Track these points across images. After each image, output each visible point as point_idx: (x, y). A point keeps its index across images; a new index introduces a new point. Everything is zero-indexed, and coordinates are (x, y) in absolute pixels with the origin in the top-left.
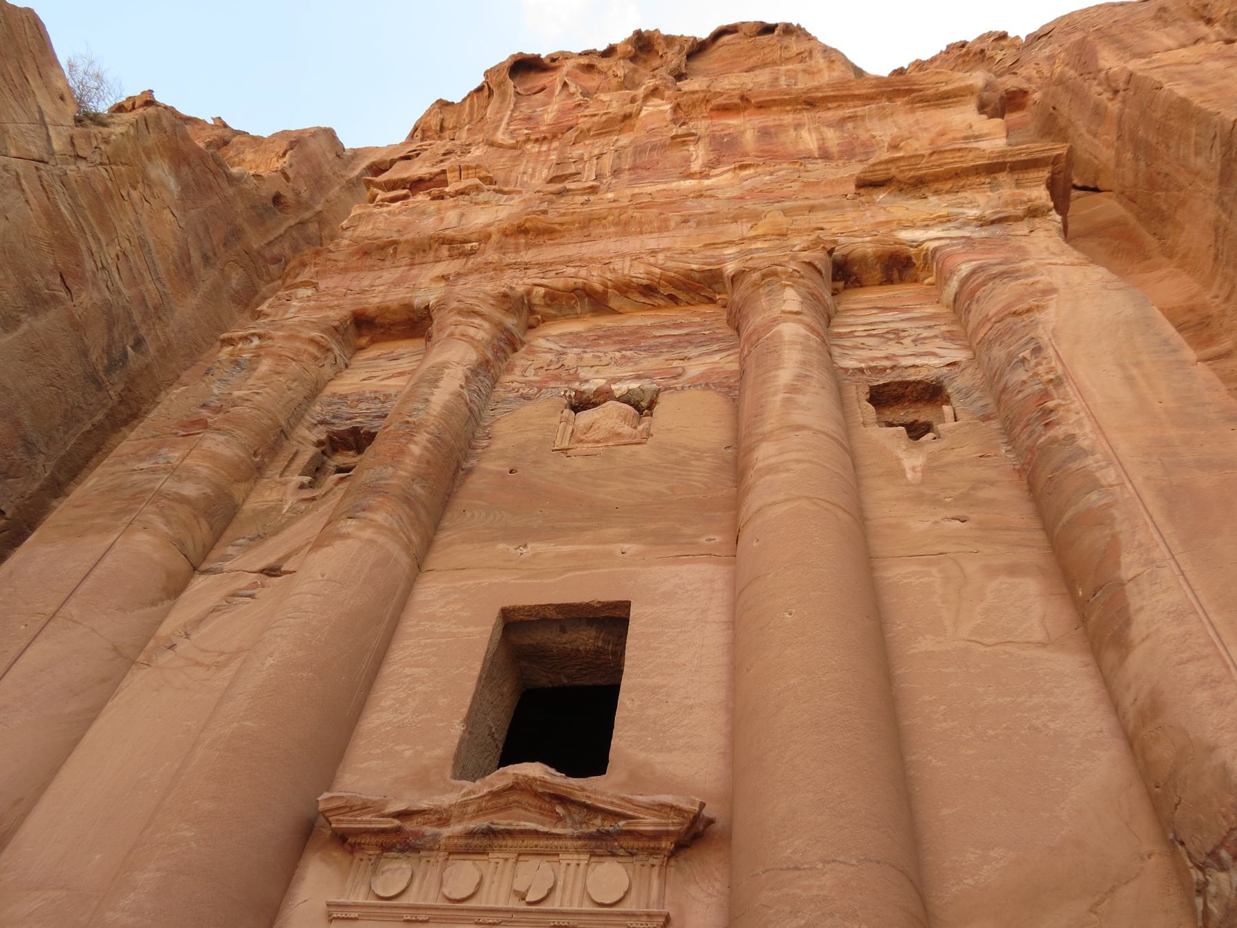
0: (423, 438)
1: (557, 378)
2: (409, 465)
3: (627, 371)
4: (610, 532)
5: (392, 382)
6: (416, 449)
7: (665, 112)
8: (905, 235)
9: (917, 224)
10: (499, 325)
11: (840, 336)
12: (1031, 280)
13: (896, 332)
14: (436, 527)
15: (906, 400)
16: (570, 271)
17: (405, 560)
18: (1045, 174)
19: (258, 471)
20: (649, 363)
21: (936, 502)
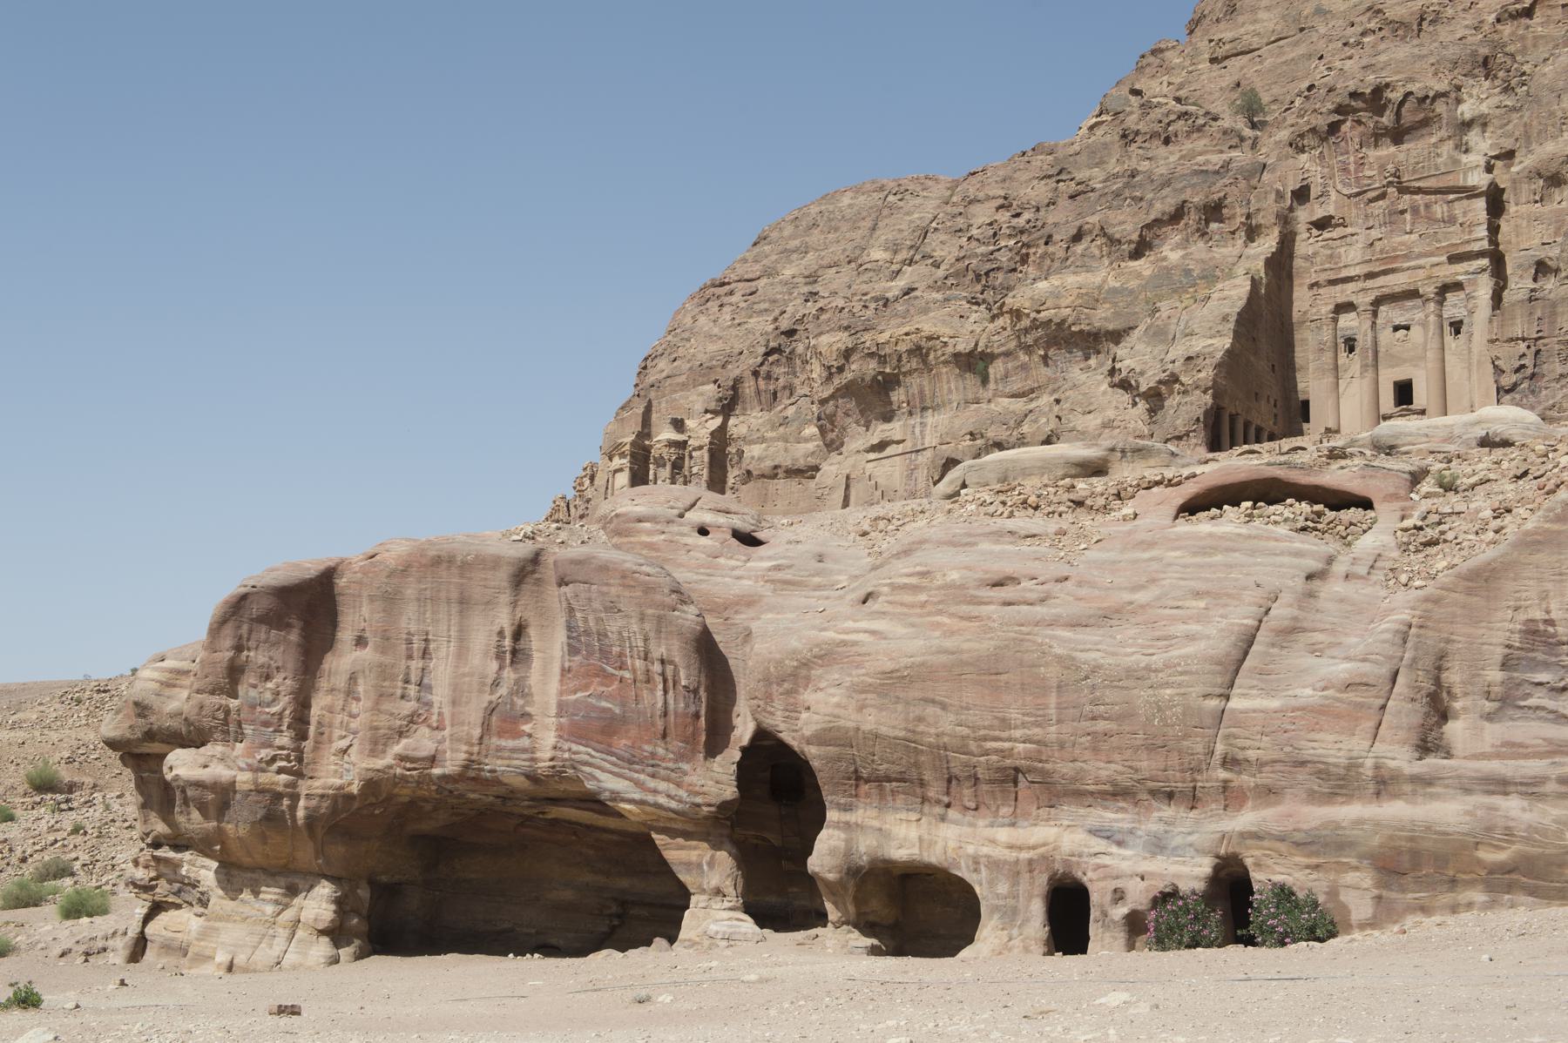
9: (1460, 271)
15: (1457, 327)
20: (1408, 316)
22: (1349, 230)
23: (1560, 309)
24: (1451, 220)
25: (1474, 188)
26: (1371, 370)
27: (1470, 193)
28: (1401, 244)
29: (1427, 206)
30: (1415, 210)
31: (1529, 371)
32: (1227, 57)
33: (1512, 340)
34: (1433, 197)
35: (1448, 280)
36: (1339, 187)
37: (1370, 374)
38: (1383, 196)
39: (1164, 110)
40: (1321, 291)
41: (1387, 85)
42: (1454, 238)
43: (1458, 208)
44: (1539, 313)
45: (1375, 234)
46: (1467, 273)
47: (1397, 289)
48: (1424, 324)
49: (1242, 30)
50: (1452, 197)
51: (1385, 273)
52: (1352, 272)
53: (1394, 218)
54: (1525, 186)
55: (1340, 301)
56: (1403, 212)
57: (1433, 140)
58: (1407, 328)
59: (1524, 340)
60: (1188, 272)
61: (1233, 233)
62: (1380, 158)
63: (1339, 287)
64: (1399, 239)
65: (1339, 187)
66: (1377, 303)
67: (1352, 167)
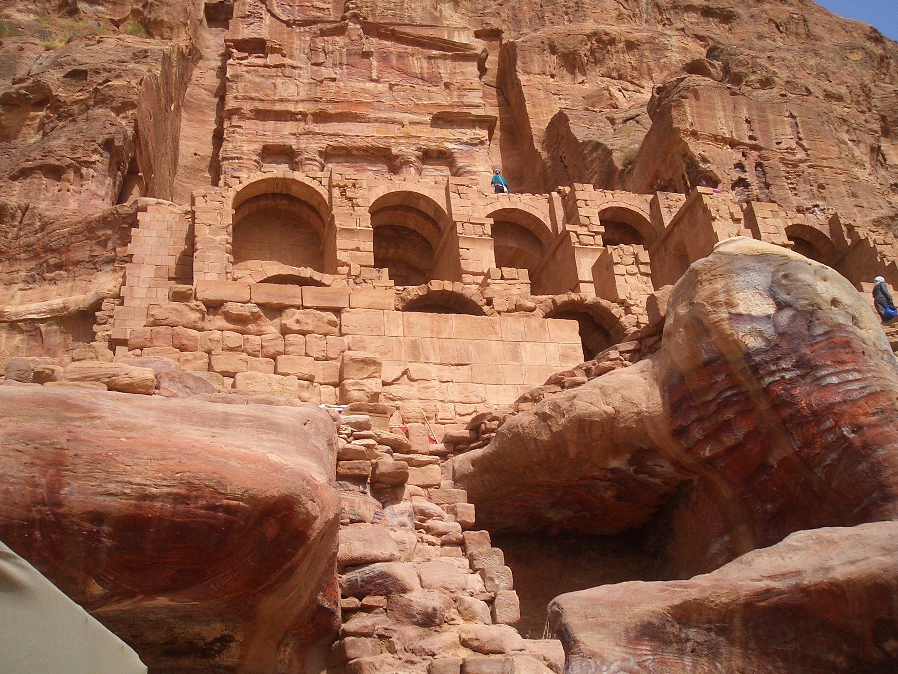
9: (449, 138)
10: (321, 163)
12: (474, 177)
16: (340, 140)
18: (488, 124)
22: (287, 61)
23: (771, 117)
25: (466, 46)
27: (460, 53)
28: (364, 90)
29: (400, 56)
30: (384, 58)
34: (410, 49)
35: (433, 146)
36: (277, 11)
38: (341, 31)
40: (242, 123)
42: (442, 99)
43: (445, 69)
44: (745, 113)
45: (327, 72)
47: (360, 143)
50: (434, 52)
51: (342, 118)
52: (291, 108)
53: (356, 60)
54: (536, 57)
55: (270, 141)
56: (367, 55)
59: (733, 144)
61: (117, 24)
63: (270, 125)
64: (361, 85)
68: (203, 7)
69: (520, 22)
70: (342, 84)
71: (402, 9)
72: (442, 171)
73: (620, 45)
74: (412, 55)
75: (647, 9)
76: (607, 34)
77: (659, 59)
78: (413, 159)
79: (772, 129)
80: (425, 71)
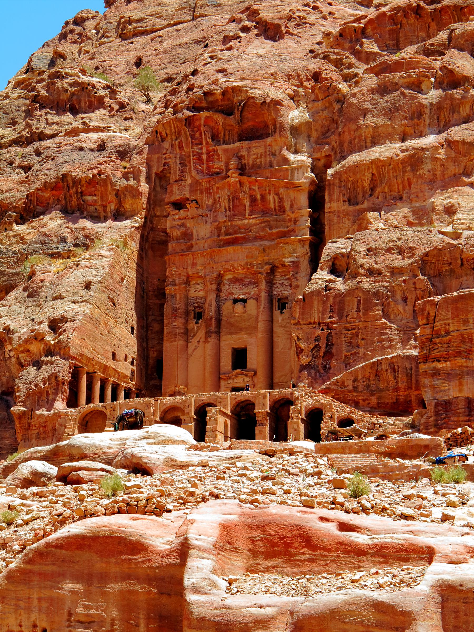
0: (213, 320)
1: (230, 294)
2: (213, 325)
3: (241, 292)
4: (243, 333)
5: (200, 293)
6: (213, 322)
7: (237, 182)
8: (284, 260)
11: (275, 284)
13: (283, 283)
14: (220, 333)
17: (218, 342)
19: (187, 321)
20: (245, 290)
21: (282, 327)
22: (201, 211)
24: (282, 209)
26: (213, 335)
27: (297, 187)
29: (263, 197)
30: (253, 200)
31: (323, 350)
32: (135, 35)
33: (310, 323)
37: (213, 340)
39: (70, 80)
41: (234, 89)
46: (290, 257)
48: (257, 298)
49: (149, 11)
57: (269, 140)
58: (244, 301)
60: (63, 240)
62: (225, 151)
65: (194, 173)
66: (220, 276)
67: (204, 157)
68: (154, 175)
69: (342, 146)
70: (229, 224)
71: (265, 156)
72: (285, 276)
73: (391, 167)
74: (270, 194)
75: (430, 113)
76: (380, 161)
77: (417, 171)
78: (264, 274)
79: (346, 307)
80: (277, 205)
